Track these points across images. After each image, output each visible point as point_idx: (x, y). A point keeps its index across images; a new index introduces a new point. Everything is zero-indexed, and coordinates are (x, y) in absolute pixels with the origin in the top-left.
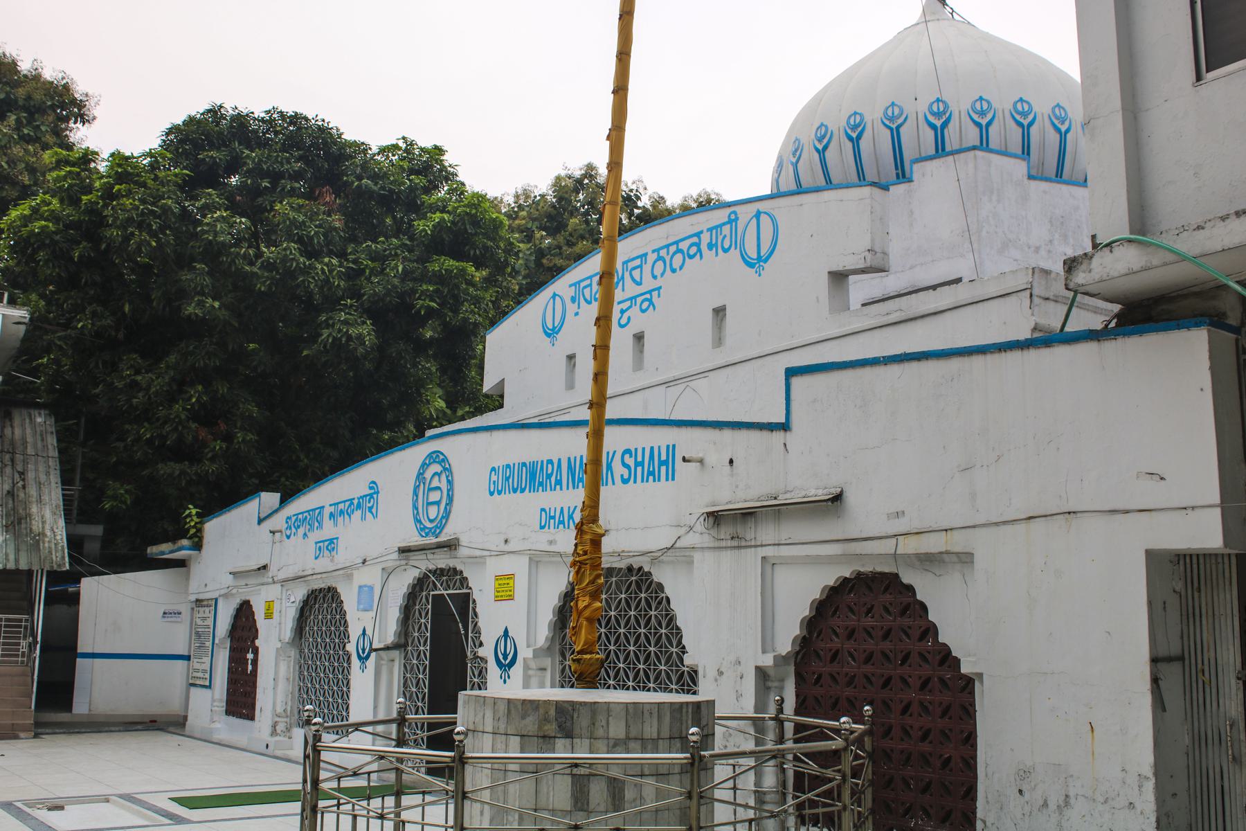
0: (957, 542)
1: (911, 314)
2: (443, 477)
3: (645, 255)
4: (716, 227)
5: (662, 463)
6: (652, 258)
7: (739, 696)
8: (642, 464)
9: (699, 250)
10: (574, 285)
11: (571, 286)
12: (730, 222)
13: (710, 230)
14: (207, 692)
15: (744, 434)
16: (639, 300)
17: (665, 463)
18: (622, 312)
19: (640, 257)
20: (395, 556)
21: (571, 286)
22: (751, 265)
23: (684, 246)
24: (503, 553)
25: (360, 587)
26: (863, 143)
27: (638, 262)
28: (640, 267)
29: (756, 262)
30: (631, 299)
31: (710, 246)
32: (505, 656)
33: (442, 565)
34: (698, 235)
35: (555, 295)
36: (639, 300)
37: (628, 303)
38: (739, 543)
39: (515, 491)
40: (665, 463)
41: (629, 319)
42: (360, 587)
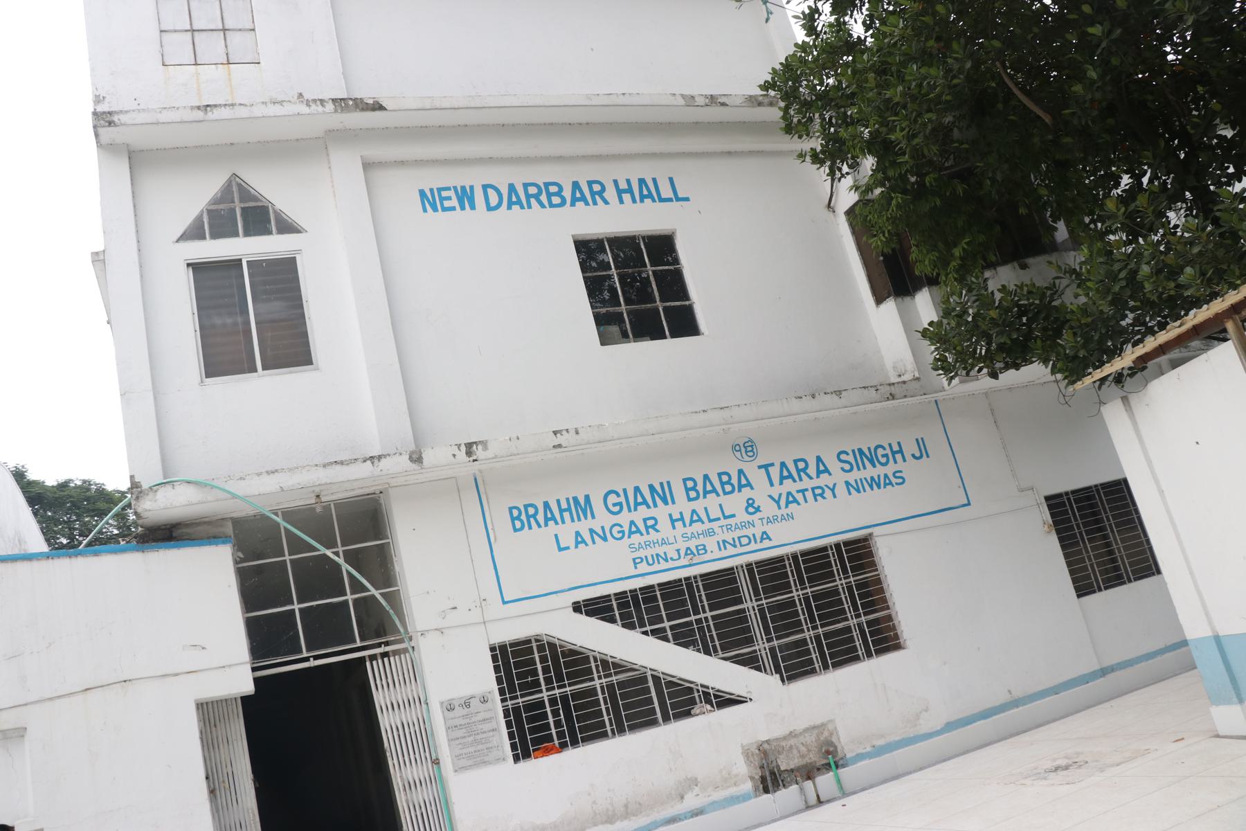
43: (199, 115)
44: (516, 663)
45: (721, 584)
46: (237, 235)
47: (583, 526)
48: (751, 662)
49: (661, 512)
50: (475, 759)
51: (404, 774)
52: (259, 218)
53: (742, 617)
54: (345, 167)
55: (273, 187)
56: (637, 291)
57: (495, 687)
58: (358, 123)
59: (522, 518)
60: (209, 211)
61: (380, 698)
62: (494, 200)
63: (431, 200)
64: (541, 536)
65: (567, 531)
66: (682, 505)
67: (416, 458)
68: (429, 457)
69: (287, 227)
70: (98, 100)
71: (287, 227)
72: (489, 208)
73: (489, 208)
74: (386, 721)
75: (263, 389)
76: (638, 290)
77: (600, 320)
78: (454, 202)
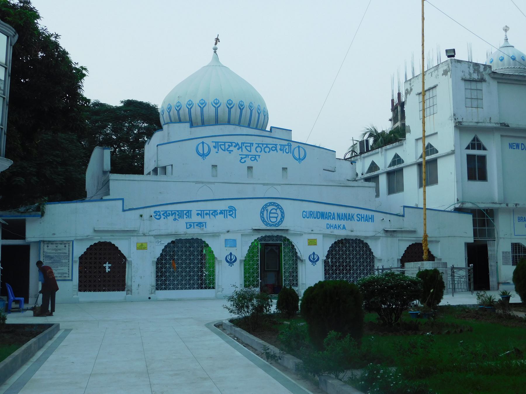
0: (438, 239)
1: (347, 185)
2: (278, 210)
3: (253, 144)
4: (283, 145)
5: (369, 218)
6: (255, 146)
7: (393, 264)
8: (364, 218)
9: (276, 148)
10: (216, 142)
11: (213, 142)
12: (288, 145)
13: (281, 145)
14: (70, 282)
15: (393, 216)
16: (250, 157)
17: (371, 218)
18: (242, 158)
19: (251, 144)
20: (251, 231)
21: (213, 142)
22: (297, 160)
23: (270, 146)
24: (311, 233)
25: (226, 240)
27: (249, 145)
28: (250, 146)
29: (300, 160)
30: (246, 155)
31: (281, 150)
32: (314, 259)
33: (280, 235)
34: (276, 145)
35: (203, 143)
36: (250, 157)
37: (245, 156)
38: (393, 236)
39: (315, 218)
40: (371, 218)
41: (245, 161)
42: (226, 240)
43: (476, 124)
46: (475, 149)
50: (505, 263)
51: (491, 263)
54: (497, 137)
55: (484, 140)
58: (504, 129)
59: (520, 219)
60: (471, 143)
61: (489, 248)
62: (523, 148)
63: (511, 146)
67: (507, 205)
68: (509, 205)
69: (484, 149)
70: (454, 115)
71: (484, 149)
72: (522, 149)
73: (522, 149)
74: (489, 253)
75: (477, 185)
78: (515, 147)
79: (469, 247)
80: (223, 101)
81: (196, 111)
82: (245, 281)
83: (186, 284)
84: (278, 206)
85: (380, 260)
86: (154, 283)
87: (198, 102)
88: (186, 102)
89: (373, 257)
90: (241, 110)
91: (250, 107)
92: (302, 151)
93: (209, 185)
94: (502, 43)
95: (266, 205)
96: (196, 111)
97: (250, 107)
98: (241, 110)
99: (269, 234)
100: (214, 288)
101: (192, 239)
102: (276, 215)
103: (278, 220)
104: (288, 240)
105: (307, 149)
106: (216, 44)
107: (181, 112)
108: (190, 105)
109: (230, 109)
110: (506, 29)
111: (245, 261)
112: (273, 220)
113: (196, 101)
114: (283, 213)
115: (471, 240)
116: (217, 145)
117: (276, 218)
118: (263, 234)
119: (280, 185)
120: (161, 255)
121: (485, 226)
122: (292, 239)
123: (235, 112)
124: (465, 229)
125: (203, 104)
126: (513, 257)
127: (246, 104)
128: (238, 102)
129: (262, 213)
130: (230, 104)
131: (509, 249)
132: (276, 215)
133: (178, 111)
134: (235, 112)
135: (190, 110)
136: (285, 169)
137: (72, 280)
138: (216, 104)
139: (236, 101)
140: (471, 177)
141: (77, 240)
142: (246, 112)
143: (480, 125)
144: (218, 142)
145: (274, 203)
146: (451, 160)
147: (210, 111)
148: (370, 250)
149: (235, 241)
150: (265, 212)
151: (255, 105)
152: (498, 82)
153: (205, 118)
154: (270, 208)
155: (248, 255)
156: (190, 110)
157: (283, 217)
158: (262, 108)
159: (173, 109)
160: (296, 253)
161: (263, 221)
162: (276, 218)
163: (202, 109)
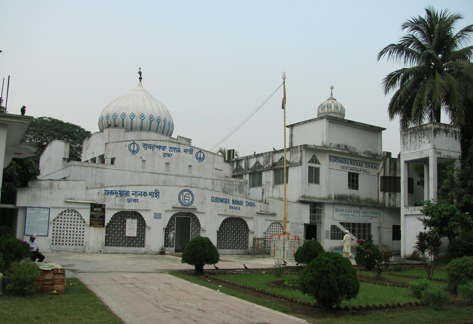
26: (160, 123)
42: (155, 214)
44: (334, 228)
45: (354, 224)
47: (342, 213)
48: (355, 235)
49: (350, 214)
50: (327, 238)
52: (317, 162)
53: (355, 230)
55: (319, 158)
56: (353, 180)
57: (330, 230)
61: (318, 228)
64: (338, 213)
65: (341, 213)
66: (352, 214)
69: (319, 163)
71: (319, 163)
75: (314, 186)
76: (353, 181)
77: (349, 185)
79: (307, 226)
80: (147, 115)
81: (127, 120)
82: (165, 243)
83: (120, 243)
84: (190, 193)
85: (253, 233)
86: (104, 241)
87: (129, 114)
88: (121, 114)
89: (249, 230)
90: (159, 123)
91: (165, 121)
92: (202, 154)
93: (139, 174)
94: (329, 96)
95: (182, 191)
96: (127, 120)
97: (165, 121)
98: (159, 123)
99: (183, 211)
100: (144, 246)
101: (132, 211)
102: (188, 198)
103: (190, 201)
104: (195, 216)
105: (205, 153)
106: (141, 75)
107: (117, 120)
108: (124, 115)
109: (151, 121)
110: (332, 88)
111: (166, 229)
112: (187, 201)
113: (128, 114)
114: (193, 197)
115: (308, 222)
116: (145, 146)
117: (189, 200)
118: (179, 211)
119: (186, 176)
120: (110, 221)
121: (316, 213)
122: (198, 216)
123: (154, 124)
124: (305, 215)
125: (133, 116)
126: (331, 234)
127: (162, 119)
128: (157, 117)
129: (179, 196)
130: (151, 118)
131: (329, 229)
132: (188, 198)
133: (114, 120)
134: (154, 124)
135: (123, 119)
136: (190, 166)
137: (47, 236)
138: (142, 116)
139: (156, 116)
140: (310, 181)
141: (53, 207)
142: (162, 124)
143: (317, 147)
144: (147, 144)
145: (188, 190)
146: (300, 168)
147: (137, 121)
148: (247, 225)
149: (161, 214)
150: (182, 196)
151: (168, 121)
152: (329, 122)
153: (134, 126)
154: (185, 193)
155: (168, 225)
156: (123, 119)
157: (193, 200)
158: (171, 123)
159: (111, 117)
160: (200, 225)
161: (180, 202)
162: (189, 200)
163: (132, 120)
